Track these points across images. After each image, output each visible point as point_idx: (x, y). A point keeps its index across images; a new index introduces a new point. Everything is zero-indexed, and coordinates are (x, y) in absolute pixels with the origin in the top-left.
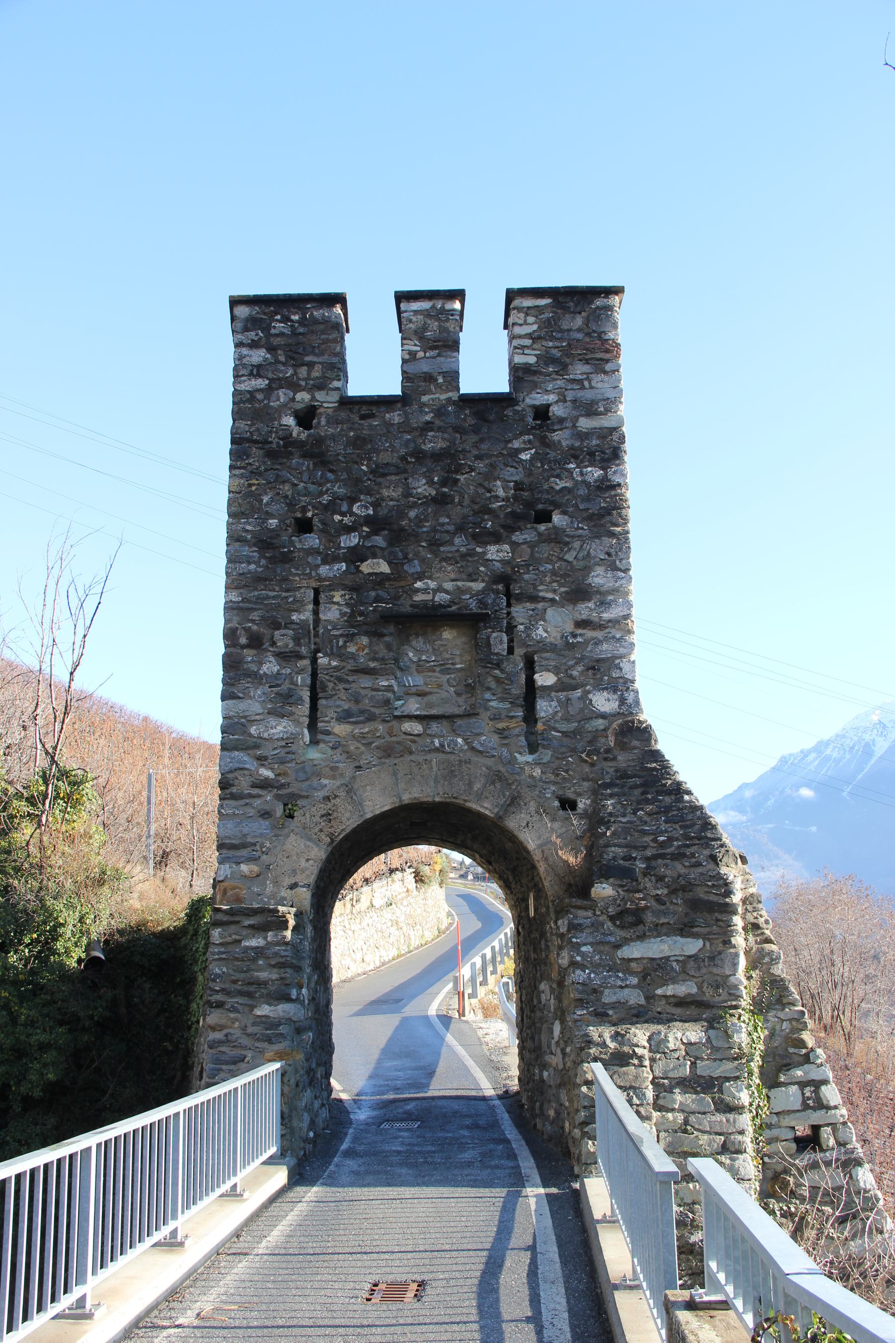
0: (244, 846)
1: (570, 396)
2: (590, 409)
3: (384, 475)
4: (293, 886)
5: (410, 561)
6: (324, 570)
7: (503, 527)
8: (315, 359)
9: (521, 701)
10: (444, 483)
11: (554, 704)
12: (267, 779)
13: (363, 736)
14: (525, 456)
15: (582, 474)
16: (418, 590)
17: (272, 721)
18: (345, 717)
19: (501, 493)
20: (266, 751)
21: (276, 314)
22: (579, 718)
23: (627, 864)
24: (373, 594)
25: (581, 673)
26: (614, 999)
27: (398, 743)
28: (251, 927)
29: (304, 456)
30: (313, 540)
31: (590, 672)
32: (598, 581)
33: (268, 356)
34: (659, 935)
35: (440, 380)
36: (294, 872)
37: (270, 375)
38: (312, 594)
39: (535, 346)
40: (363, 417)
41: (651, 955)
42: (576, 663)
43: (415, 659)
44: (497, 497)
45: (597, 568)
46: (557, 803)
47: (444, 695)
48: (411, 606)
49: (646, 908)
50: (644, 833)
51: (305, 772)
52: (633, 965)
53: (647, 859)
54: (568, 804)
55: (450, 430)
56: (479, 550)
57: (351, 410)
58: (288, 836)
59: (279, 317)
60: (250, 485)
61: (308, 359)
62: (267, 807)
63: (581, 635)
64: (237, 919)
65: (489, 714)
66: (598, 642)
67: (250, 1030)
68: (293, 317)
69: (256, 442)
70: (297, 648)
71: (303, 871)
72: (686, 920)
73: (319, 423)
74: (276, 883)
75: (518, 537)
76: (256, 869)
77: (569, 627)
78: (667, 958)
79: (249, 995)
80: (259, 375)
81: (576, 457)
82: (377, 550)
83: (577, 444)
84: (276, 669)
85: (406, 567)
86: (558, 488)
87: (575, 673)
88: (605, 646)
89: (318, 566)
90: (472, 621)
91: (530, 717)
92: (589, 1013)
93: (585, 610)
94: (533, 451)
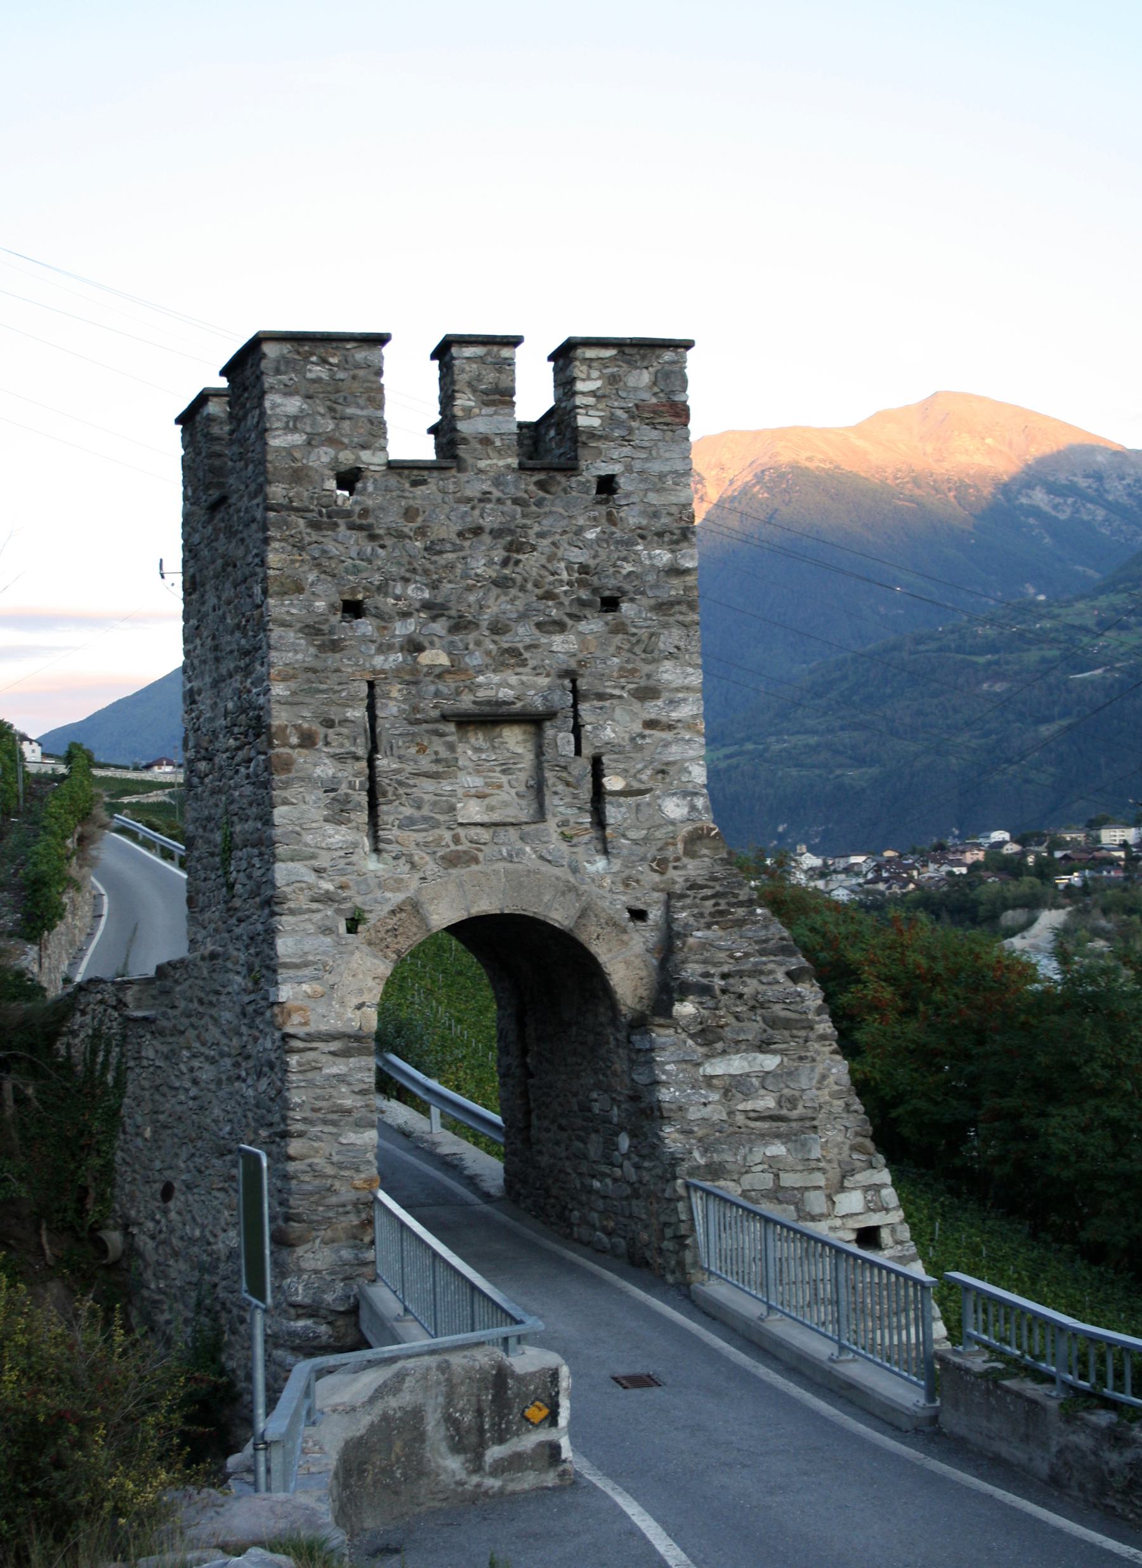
0: (306, 964)
1: (637, 465)
2: (658, 483)
3: (440, 553)
4: (359, 1007)
5: (471, 653)
6: (379, 661)
7: (570, 615)
8: (359, 412)
9: (588, 806)
10: (505, 563)
11: (623, 810)
12: (327, 892)
13: (426, 844)
14: (591, 535)
15: (650, 558)
16: (480, 686)
17: (330, 828)
18: (407, 824)
19: (565, 576)
20: (324, 861)
21: (312, 354)
22: (647, 825)
23: (705, 981)
24: (432, 688)
25: (651, 777)
26: (698, 1115)
27: (465, 852)
28: (333, 1053)
29: (352, 527)
30: (365, 626)
31: (660, 776)
32: (666, 676)
33: (305, 406)
34: (738, 1052)
35: (498, 443)
36: (361, 992)
37: (308, 430)
38: (365, 688)
39: (600, 406)
40: (415, 484)
41: (733, 1072)
42: (645, 767)
43: (474, 758)
44: (561, 581)
45: (666, 662)
46: (627, 915)
47: (503, 796)
48: (474, 702)
49: (727, 1025)
50: (720, 948)
51: (368, 885)
52: (715, 1081)
53: (724, 976)
54: (638, 915)
55: (509, 502)
56: (544, 640)
57: (400, 475)
58: (352, 953)
59: (314, 359)
60: (293, 562)
61: (350, 411)
62: (328, 923)
63: (650, 736)
64: (314, 1045)
65: (557, 820)
66: (667, 745)
67: (335, 1158)
68: (332, 360)
69: (297, 510)
70: (353, 749)
71: (370, 990)
72: (765, 1036)
73: (365, 488)
74: (342, 1003)
75: (583, 626)
76: (319, 988)
77: (637, 727)
78: (748, 1075)
79: (334, 1123)
80: (295, 430)
81: (643, 537)
82: (436, 639)
83: (644, 522)
84: (330, 772)
85: (467, 659)
86: (624, 572)
87: (644, 777)
88: (674, 748)
89: (372, 656)
90: (534, 721)
91: (600, 822)
92: (677, 1131)
93: (653, 709)
94: (598, 529)
